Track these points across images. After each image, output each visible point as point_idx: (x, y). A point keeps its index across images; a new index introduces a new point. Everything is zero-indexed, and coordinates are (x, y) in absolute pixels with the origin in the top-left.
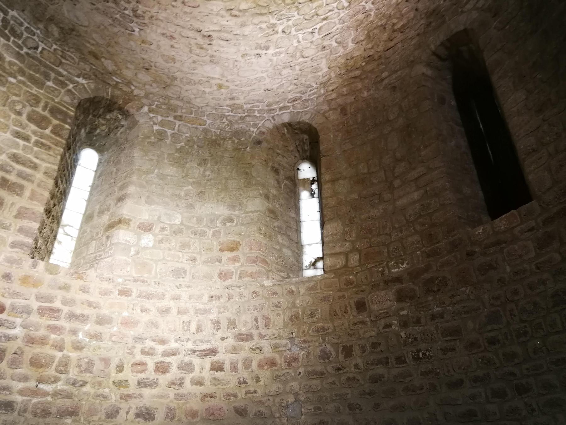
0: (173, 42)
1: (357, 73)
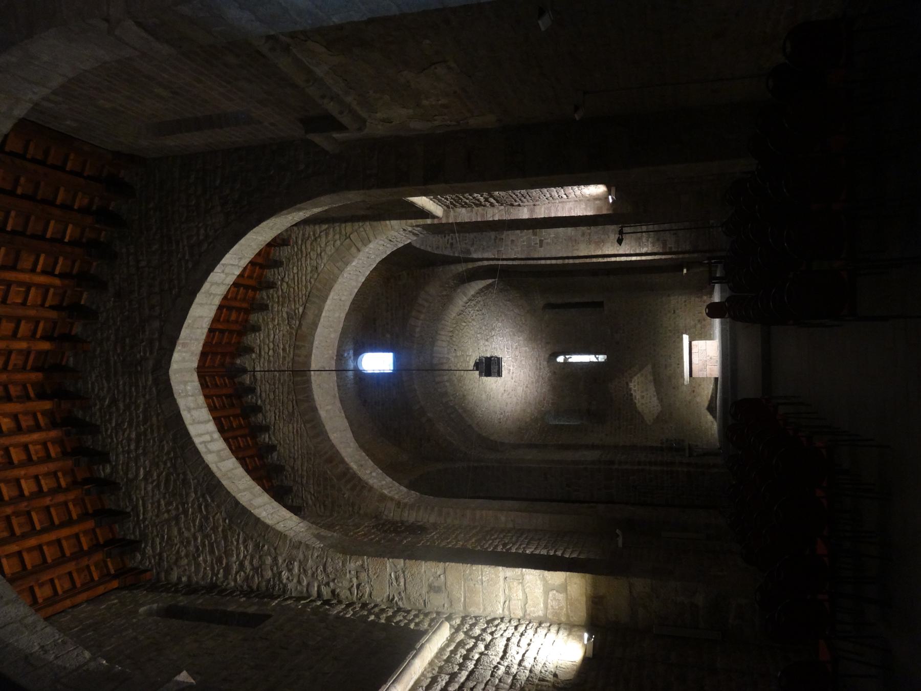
0: (509, 403)
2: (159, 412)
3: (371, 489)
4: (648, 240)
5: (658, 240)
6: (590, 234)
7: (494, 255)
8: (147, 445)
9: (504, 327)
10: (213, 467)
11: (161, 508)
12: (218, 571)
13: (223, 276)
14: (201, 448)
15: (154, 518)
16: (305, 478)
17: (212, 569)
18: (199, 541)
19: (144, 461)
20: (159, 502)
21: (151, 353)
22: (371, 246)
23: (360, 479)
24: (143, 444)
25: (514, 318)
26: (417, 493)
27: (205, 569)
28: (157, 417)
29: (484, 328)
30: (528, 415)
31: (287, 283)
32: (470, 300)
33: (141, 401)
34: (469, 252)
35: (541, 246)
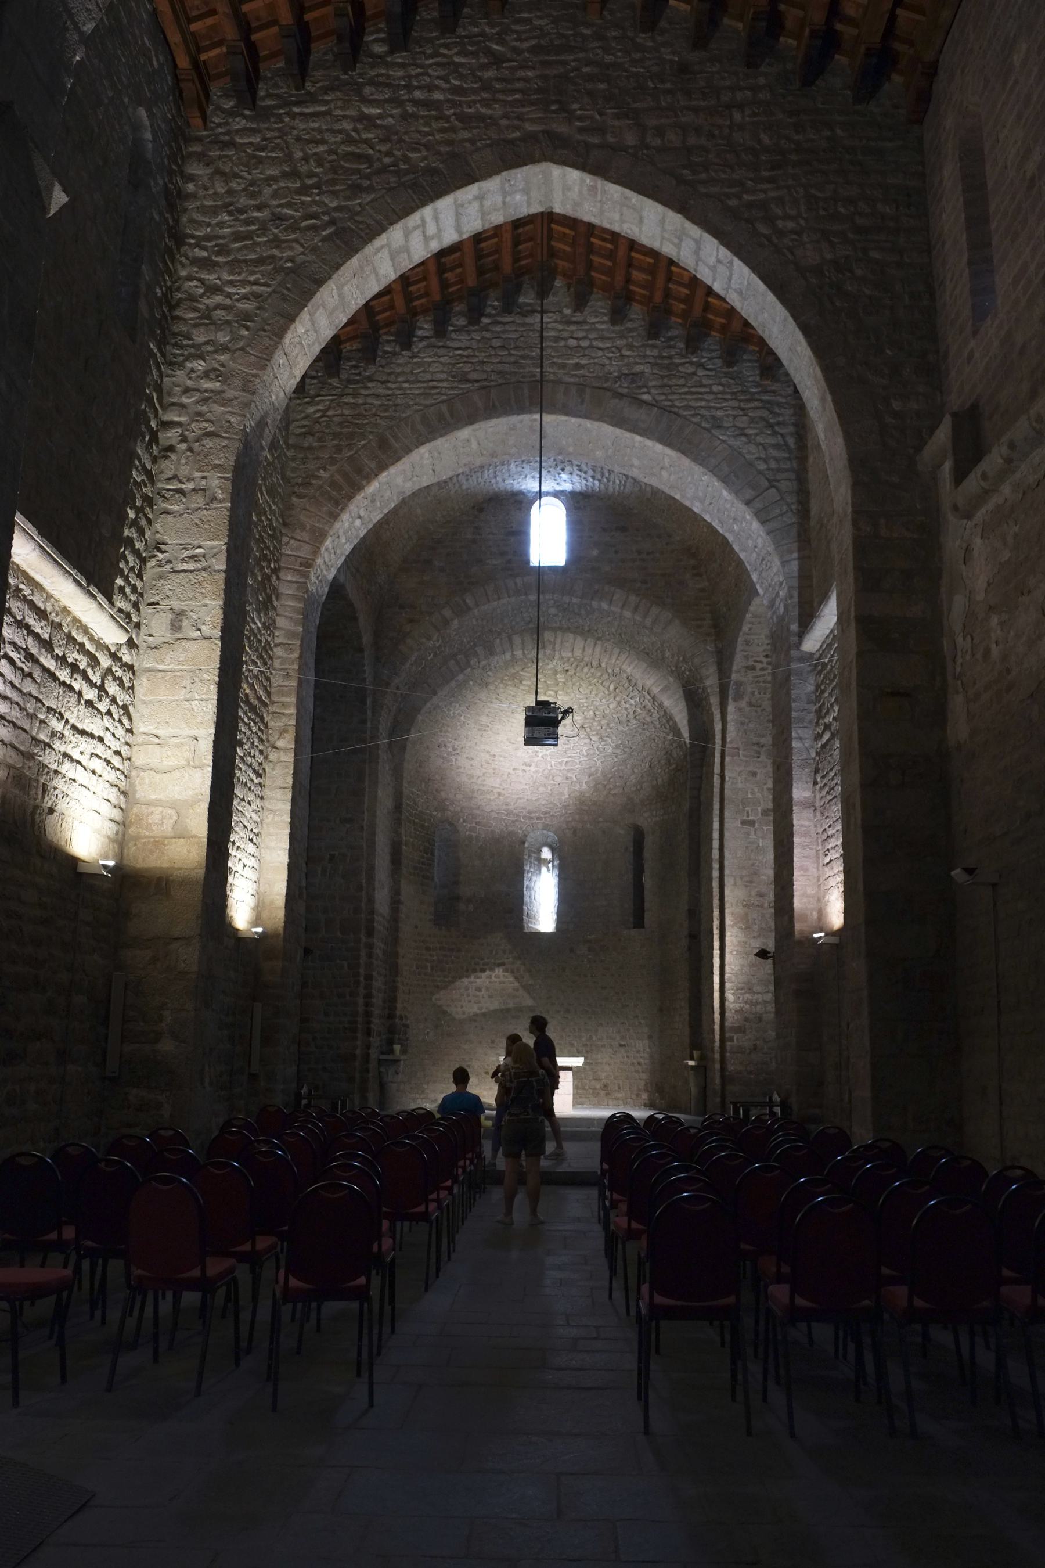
0: (472, 762)
1: (586, 808)
2: (479, 144)
3: (335, 517)
4: (746, 1003)
5: (746, 1020)
6: (762, 906)
7: (731, 742)
8: (422, 121)
9: (604, 757)
10: (380, 241)
11: (311, 146)
12: (205, 248)
13: (712, 261)
14: (414, 219)
15: (295, 132)
16: (352, 401)
17: (208, 238)
18: (256, 214)
19: (392, 116)
20: (323, 142)
21: (581, 130)
22: (756, 525)
23: (350, 497)
24: (422, 113)
25: (621, 774)
26: (324, 597)
27: (209, 225)
28: (469, 140)
29: (604, 722)
30: (451, 796)
31: (694, 374)
32: (654, 698)
33: (497, 110)
34: (738, 697)
35: (743, 823)
